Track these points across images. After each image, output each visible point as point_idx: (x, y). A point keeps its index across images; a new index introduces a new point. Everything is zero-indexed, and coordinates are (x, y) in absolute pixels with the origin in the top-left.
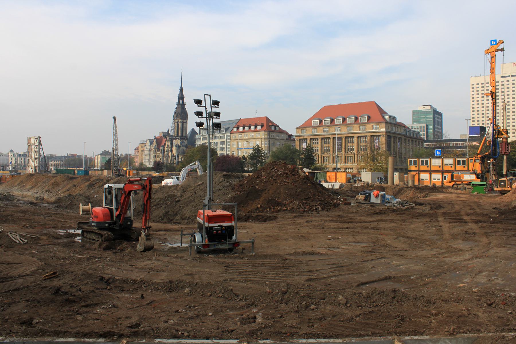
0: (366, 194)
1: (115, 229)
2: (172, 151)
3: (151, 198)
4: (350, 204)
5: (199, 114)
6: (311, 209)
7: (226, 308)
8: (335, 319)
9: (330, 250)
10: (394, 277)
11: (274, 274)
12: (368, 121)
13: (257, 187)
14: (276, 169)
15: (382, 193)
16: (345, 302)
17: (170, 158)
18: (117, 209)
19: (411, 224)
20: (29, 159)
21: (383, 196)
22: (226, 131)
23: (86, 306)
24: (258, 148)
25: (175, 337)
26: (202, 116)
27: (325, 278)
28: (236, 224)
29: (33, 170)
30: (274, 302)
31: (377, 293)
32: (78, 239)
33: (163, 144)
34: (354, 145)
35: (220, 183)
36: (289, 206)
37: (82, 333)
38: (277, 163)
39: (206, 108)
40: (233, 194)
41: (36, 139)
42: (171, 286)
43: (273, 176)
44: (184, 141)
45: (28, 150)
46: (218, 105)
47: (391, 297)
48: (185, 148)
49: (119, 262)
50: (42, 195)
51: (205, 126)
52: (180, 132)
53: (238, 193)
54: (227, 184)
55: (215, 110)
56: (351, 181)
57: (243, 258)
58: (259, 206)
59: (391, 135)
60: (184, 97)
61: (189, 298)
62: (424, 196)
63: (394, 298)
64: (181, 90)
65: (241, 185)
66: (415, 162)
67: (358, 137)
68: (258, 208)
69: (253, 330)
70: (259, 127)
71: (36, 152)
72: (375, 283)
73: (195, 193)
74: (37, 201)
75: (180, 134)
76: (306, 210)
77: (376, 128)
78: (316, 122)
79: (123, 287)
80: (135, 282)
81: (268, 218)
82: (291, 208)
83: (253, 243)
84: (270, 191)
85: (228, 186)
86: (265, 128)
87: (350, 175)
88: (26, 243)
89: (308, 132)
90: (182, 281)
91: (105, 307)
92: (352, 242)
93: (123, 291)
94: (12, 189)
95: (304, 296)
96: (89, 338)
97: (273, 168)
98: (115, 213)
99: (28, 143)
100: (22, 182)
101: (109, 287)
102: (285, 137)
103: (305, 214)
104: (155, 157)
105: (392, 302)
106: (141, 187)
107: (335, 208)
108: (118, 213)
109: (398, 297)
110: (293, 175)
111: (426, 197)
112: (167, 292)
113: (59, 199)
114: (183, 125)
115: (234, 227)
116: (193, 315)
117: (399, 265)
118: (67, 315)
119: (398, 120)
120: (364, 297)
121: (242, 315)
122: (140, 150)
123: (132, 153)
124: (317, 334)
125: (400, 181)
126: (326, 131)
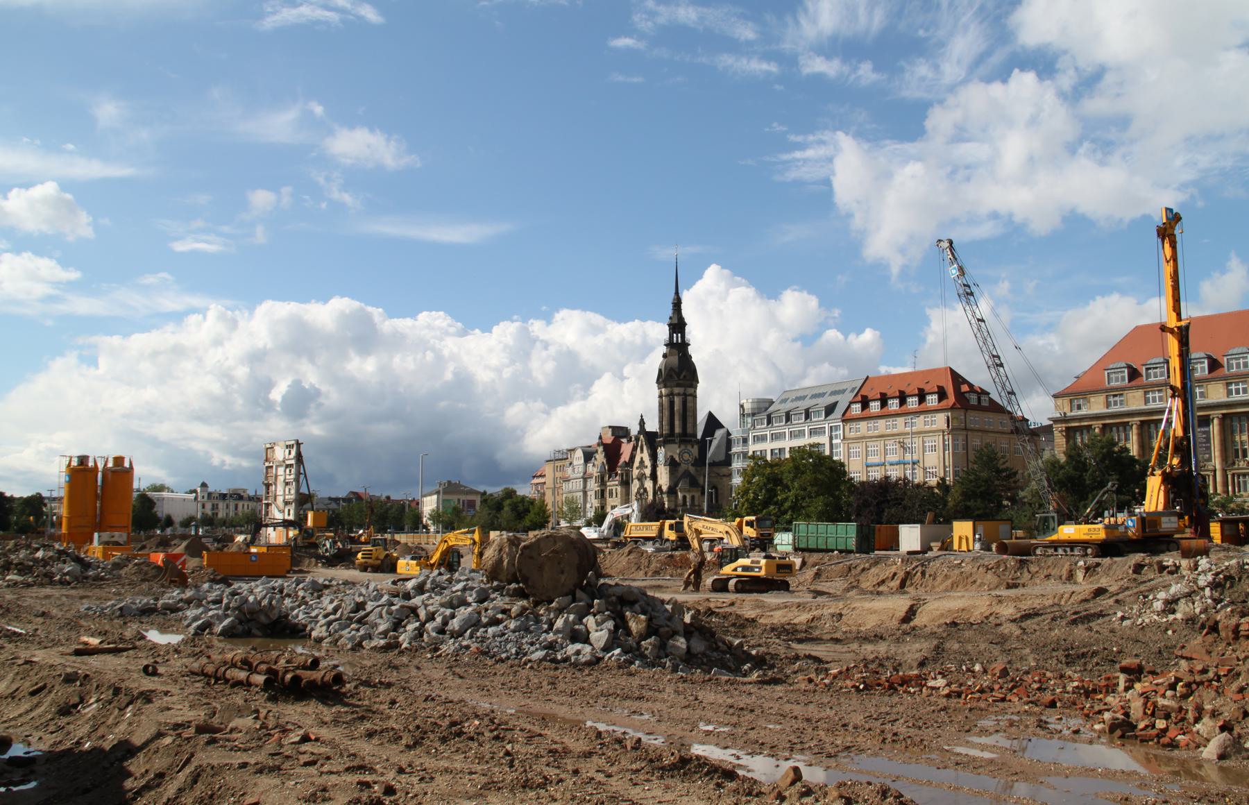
2: (654, 477)
20: (268, 505)
22: (826, 416)
33: (625, 457)
44: (689, 447)
45: (267, 478)
52: (677, 423)
70: (932, 400)
71: (287, 484)
75: (677, 430)
89: (1096, 406)
99: (267, 460)
126: (1154, 400)
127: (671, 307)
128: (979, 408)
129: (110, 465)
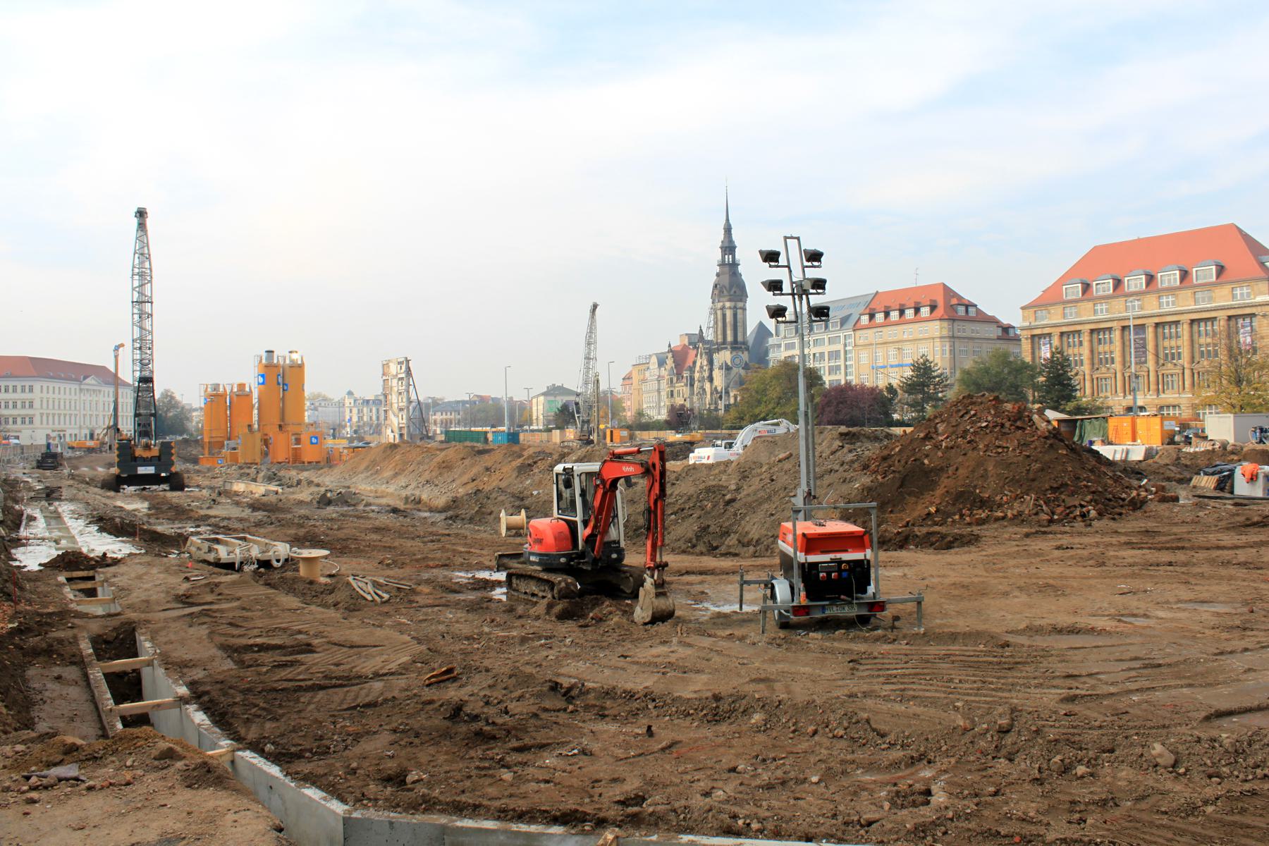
2: (711, 379)
3: (665, 495)
4: (1176, 499)
5: (775, 286)
6: (1068, 514)
7: (854, 766)
8: (1143, 805)
9: (1126, 622)
11: (975, 682)
13: (926, 461)
14: (974, 415)
16: (1172, 762)
17: (709, 396)
18: (585, 523)
20: (386, 411)
22: (842, 325)
23: (519, 750)
24: (924, 364)
25: (729, 832)
26: (781, 289)
27: (1112, 694)
28: (876, 557)
29: (397, 436)
30: (978, 755)
32: (499, 594)
33: (689, 363)
34: (1179, 343)
37: (514, 810)
38: (974, 399)
39: (790, 271)
40: (866, 480)
43: (966, 431)
44: (740, 353)
45: (384, 389)
48: (742, 372)
49: (593, 647)
50: (417, 493)
51: (789, 315)
53: (879, 477)
54: (850, 457)
55: (813, 273)
56: (1177, 438)
57: (895, 640)
58: (933, 509)
60: (735, 247)
61: (761, 737)
64: (728, 230)
65: (885, 459)
67: (1192, 321)
68: (929, 514)
70: (925, 311)
71: (400, 393)
73: (772, 480)
74: (408, 506)
76: (1056, 517)
77: (1242, 294)
78: (1075, 290)
79: (603, 708)
80: (630, 695)
81: (957, 539)
82: (1015, 512)
83: (919, 603)
84: (960, 471)
85: (852, 462)
86: (940, 311)
87: (1173, 423)
88: (387, 601)
89: (1054, 318)
91: (564, 753)
92: (1186, 602)
93: (603, 716)
94: (354, 480)
95: (1056, 740)
96: (529, 823)
97: (966, 413)
98: (583, 533)
99: (384, 374)
100: (374, 463)
101: (571, 707)
102: (995, 332)
103: (1054, 528)
104: (672, 395)
106: (641, 470)
107: (1134, 510)
108: (588, 531)
110: (1018, 428)
112: (708, 721)
114: (735, 315)
115: (872, 564)
116: (772, 781)
118: (478, 768)
121: (895, 785)
123: (618, 387)
124: (1096, 844)
127: (722, 232)
128: (967, 319)
129: (235, 390)
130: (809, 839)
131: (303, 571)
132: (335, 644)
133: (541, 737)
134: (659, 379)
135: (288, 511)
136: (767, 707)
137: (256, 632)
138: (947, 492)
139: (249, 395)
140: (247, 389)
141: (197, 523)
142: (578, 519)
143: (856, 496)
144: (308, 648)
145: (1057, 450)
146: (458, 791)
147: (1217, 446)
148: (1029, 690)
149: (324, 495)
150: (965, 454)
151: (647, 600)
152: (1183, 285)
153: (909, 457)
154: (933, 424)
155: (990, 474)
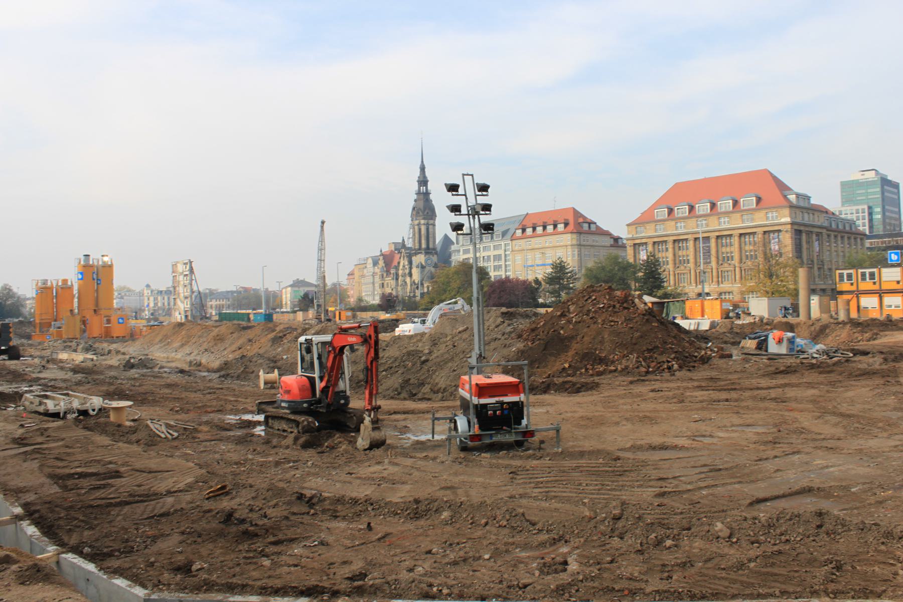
0: (759, 337)
1: (319, 411)
2: (410, 275)
3: (378, 358)
4: (730, 356)
5: (455, 209)
6: (659, 367)
7: (514, 546)
8: (709, 565)
9: (698, 441)
10: (818, 489)
11: (597, 485)
12: (757, 205)
13: (562, 332)
14: (595, 299)
15: (790, 335)
18: (321, 378)
19: (847, 391)
20: (175, 299)
21: (791, 341)
22: (503, 236)
24: (560, 264)
27: (689, 490)
29: (183, 317)
30: (600, 535)
31: (788, 517)
32: (259, 430)
33: (395, 263)
34: (732, 249)
35: (497, 326)
36: (621, 364)
37: (272, 587)
38: (595, 288)
39: (467, 199)
40: (520, 345)
41: (185, 264)
42: (417, 508)
43: (589, 311)
44: (431, 256)
45: (173, 283)
46: (487, 191)
47: (814, 526)
48: (433, 270)
49: (328, 467)
50: (198, 358)
51: (466, 230)
53: (529, 343)
54: (509, 329)
55: (482, 200)
56: (731, 314)
57: (541, 457)
58: (567, 365)
59: (802, 228)
60: (427, 181)
61: (449, 528)
62: (870, 338)
63: (819, 527)
64: (423, 169)
65: (533, 330)
66: (850, 277)
67: (741, 235)
68: (564, 369)
69: (563, 585)
70: (561, 227)
72: (783, 500)
73: (455, 346)
74: (191, 368)
76: (651, 369)
77: (772, 217)
79: (336, 511)
80: (355, 501)
81: (583, 386)
82: (623, 367)
83: (558, 431)
84: (585, 338)
85: (511, 333)
86: (571, 227)
87: (729, 304)
89: (649, 231)
90: (437, 500)
91: (308, 544)
92: (738, 426)
93: (336, 517)
94: (150, 350)
95: (652, 523)
97: (589, 298)
98: (319, 385)
99: (173, 272)
100: (166, 337)
101: (312, 511)
102: (609, 242)
103: (650, 377)
104: (383, 286)
105: (817, 535)
106: (361, 340)
108: (323, 384)
109: (828, 526)
110: (625, 308)
111: (874, 339)
113: (226, 364)
114: (428, 230)
115: (525, 404)
116: (457, 560)
117: (827, 467)
118: (245, 558)
119: (813, 201)
120: (763, 526)
121: (543, 558)
122: (357, 274)
123: (344, 281)
124: (679, 593)
125: (821, 312)
128: (589, 233)
129: (60, 284)
130: (483, 599)
131: (113, 417)
132: (137, 471)
133: (290, 534)
134: (374, 275)
135: (101, 373)
136: (452, 507)
137: (76, 464)
138: (576, 353)
139: (70, 288)
140: (69, 283)
141: (30, 384)
142: (316, 375)
143: (513, 356)
144: (117, 475)
145: (652, 323)
146: (230, 575)
147: (757, 320)
148: (633, 489)
149: (129, 361)
150: (588, 327)
151: (367, 433)
152: (735, 210)
153: (550, 329)
154: (566, 306)
155: (606, 340)
